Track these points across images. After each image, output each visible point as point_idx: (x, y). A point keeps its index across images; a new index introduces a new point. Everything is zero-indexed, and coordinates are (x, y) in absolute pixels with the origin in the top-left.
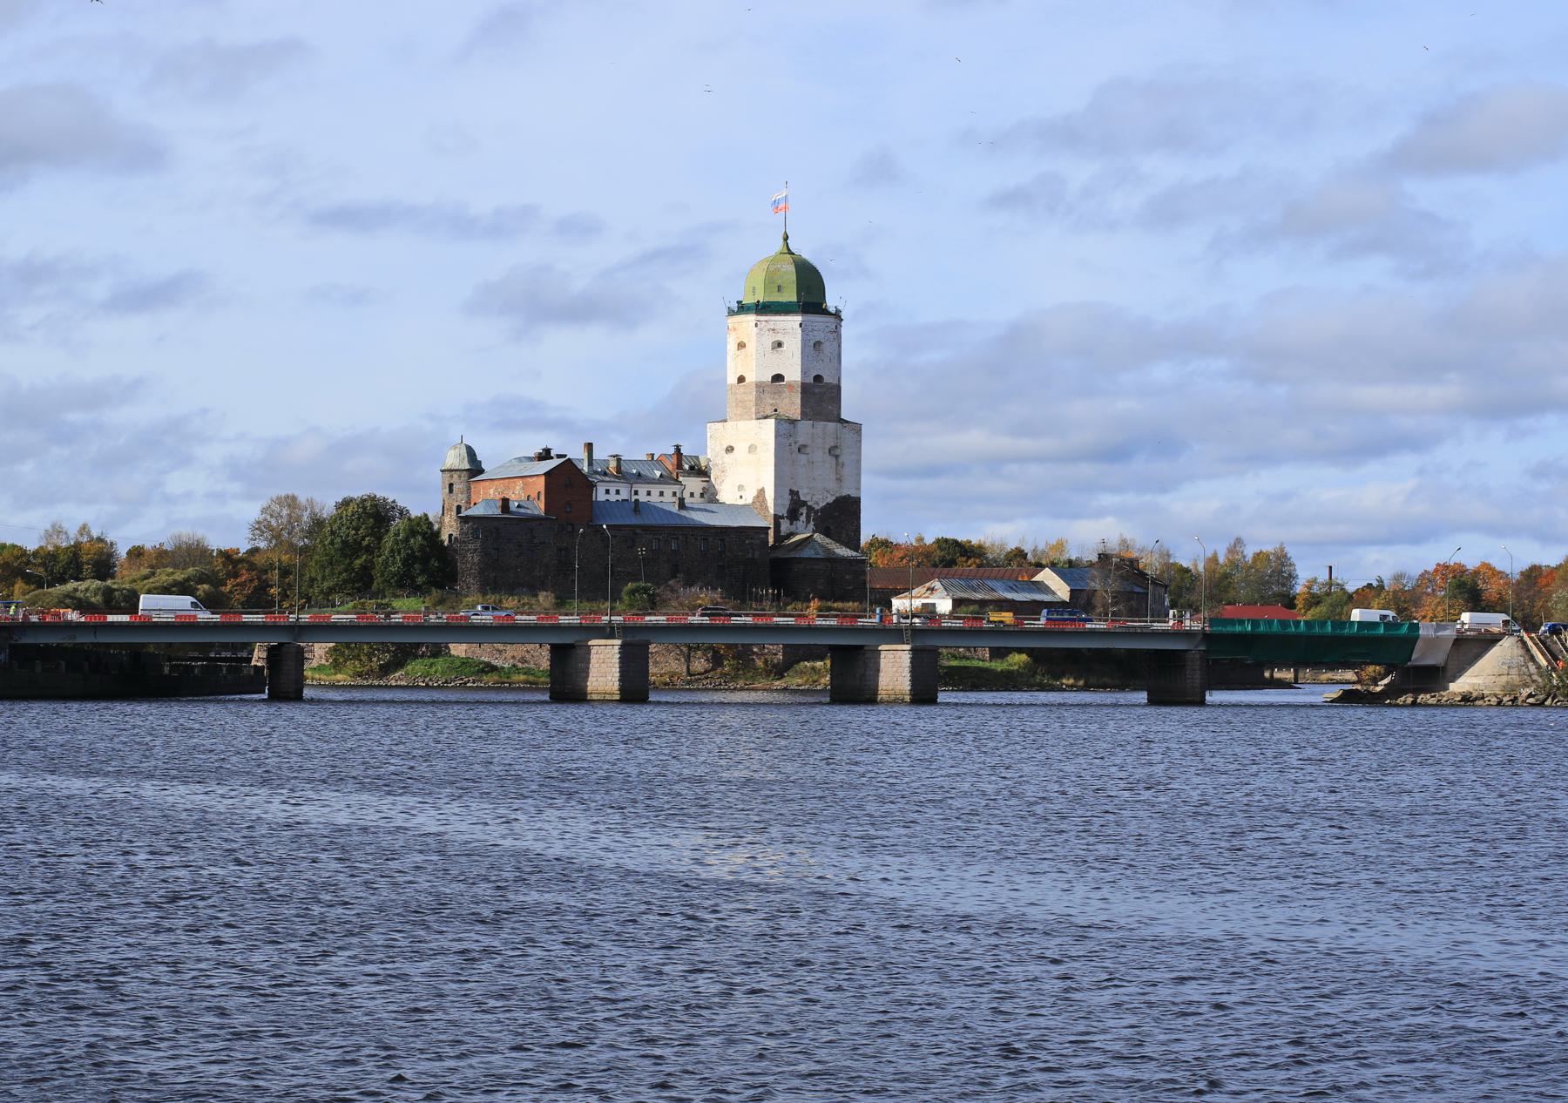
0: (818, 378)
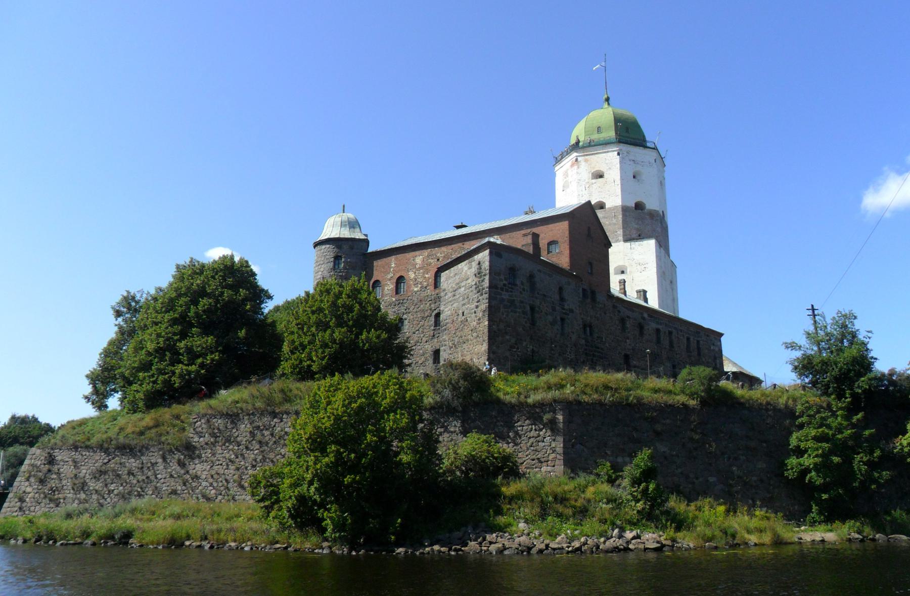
0: (663, 212)
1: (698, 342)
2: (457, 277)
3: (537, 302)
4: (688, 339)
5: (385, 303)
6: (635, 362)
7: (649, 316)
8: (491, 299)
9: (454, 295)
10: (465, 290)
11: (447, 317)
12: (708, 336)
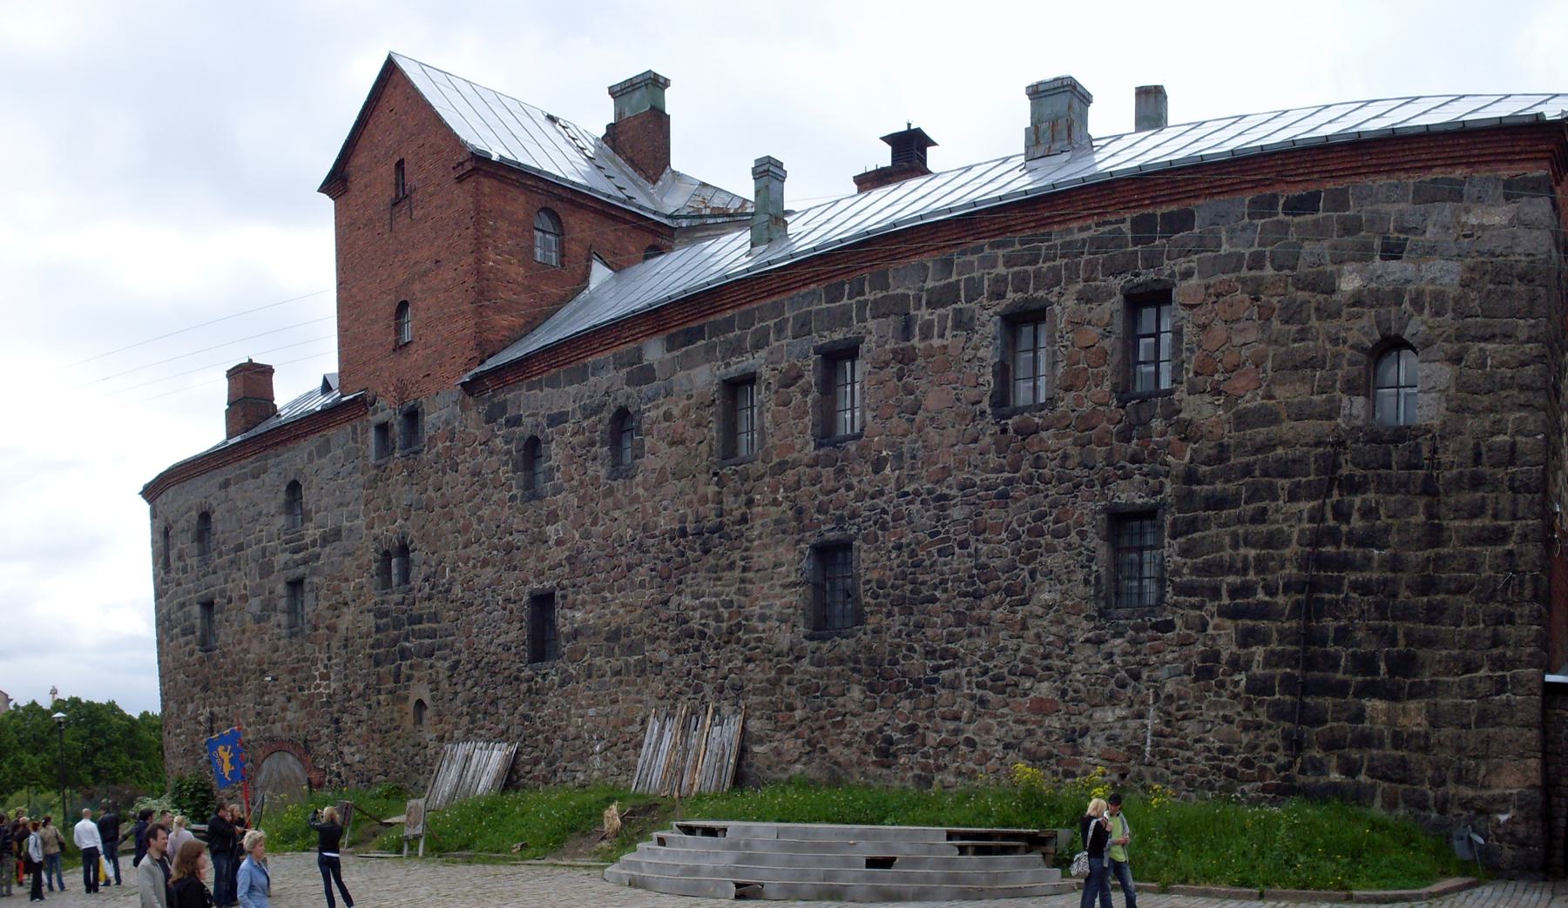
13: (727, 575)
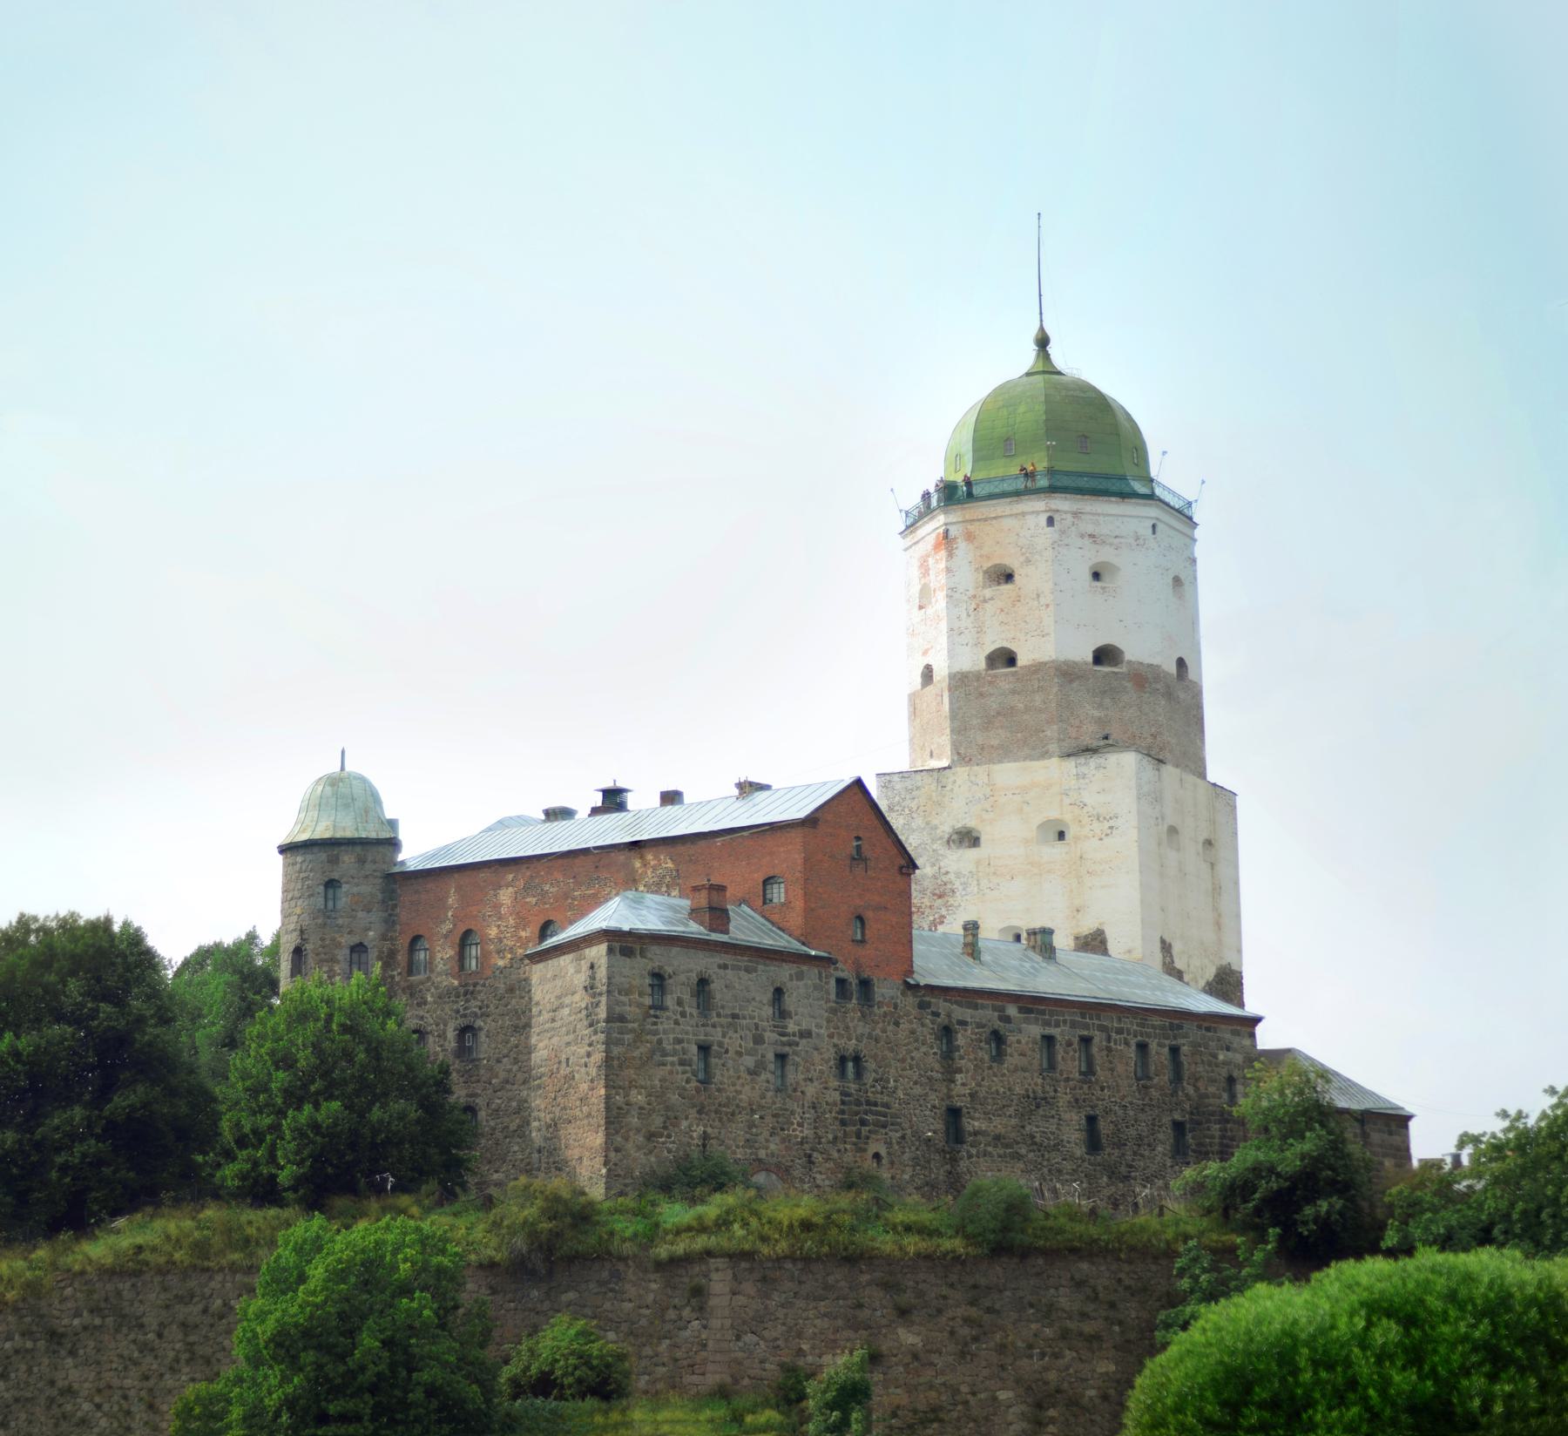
0: (1181, 663)
1: (1175, 1051)
2: (559, 982)
3: (716, 1035)
4: (1142, 1048)
5: (437, 988)
6: (976, 1124)
7: (1021, 1010)
8: (608, 1043)
9: (553, 1020)
10: (569, 1015)
11: (542, 1060)
12: (1208, 1029)
13: (1051, 1120)
